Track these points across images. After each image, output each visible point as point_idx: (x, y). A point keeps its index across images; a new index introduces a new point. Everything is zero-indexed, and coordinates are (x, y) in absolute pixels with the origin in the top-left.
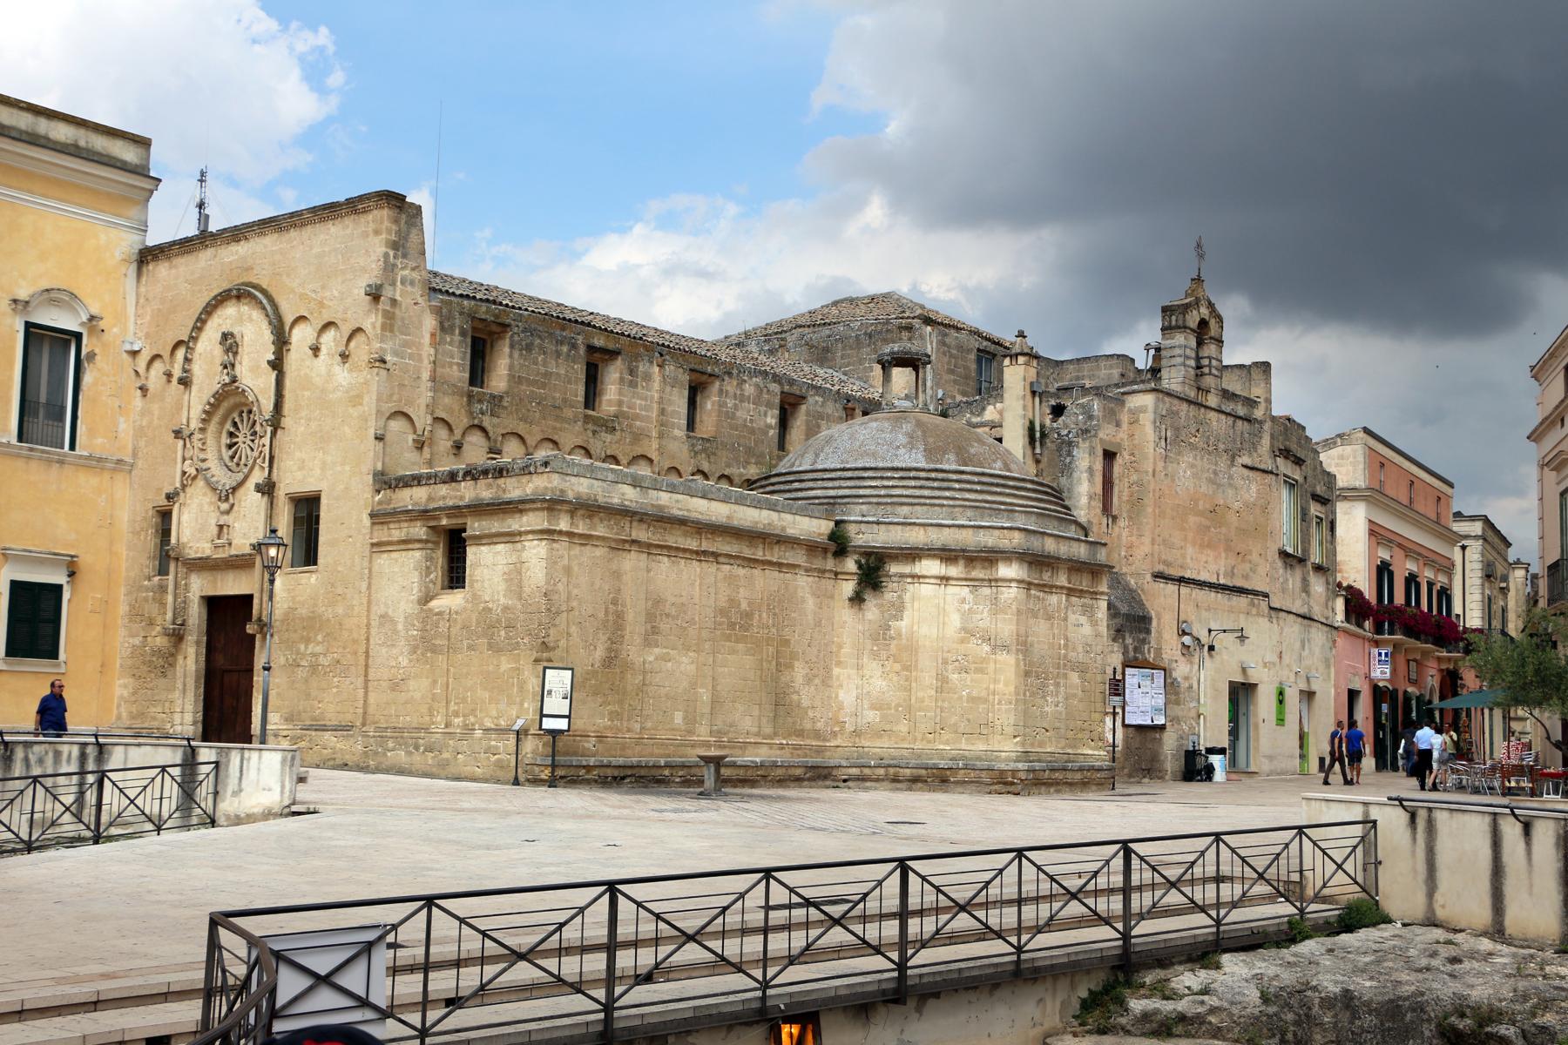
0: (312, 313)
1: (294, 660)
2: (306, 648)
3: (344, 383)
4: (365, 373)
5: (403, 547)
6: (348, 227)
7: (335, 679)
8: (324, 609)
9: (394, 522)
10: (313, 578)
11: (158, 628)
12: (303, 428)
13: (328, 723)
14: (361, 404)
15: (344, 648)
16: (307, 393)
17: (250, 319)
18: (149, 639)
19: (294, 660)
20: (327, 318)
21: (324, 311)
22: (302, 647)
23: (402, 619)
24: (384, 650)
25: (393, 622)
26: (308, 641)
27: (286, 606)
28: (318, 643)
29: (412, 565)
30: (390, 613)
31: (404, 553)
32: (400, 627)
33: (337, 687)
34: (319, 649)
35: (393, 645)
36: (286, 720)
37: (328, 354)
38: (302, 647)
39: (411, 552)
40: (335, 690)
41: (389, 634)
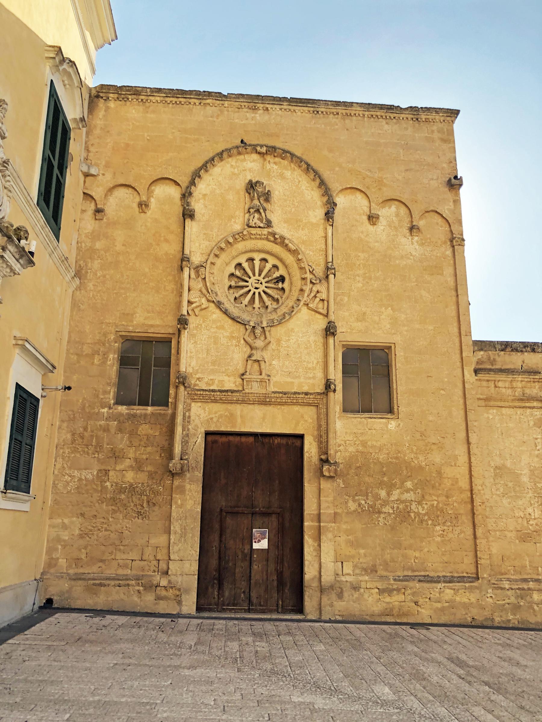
0: (368, 188)
1: (370, 506)
2: (389, 494)
3: (414, 253)
4: (443, 249)
5: (517, 404)
6: (406, 129)
7: (438, 528)
8: (412, 456)
9: (505, 381)
10: (392, 425)
11: (128, 462)
12: (360, 285)
13: (432, 574)
14: (442, 274)
15: (447, 497)
16: (362, 255)
17: (282, 176)
18: (111, 473)
19: (370, 506)
20: (389, 193)
21: (385, 189)
22: (383, 493)
23: (526, 471)
24: (505, 501)
25: (516, 477)
26: (390, 487)
27: (351, 449)
28: (408, 491)
29: (532, 423)
30: (508, 464)
31: (519, 411)
32: (525, 479)
33: (442, 536)
34: (407, 496)
35: (518, 497)
36: (365, 570)
37: (390, 226)
38: (383, 493)
39: (528, 411)
40: (439, 539)
41: (510, 484)
